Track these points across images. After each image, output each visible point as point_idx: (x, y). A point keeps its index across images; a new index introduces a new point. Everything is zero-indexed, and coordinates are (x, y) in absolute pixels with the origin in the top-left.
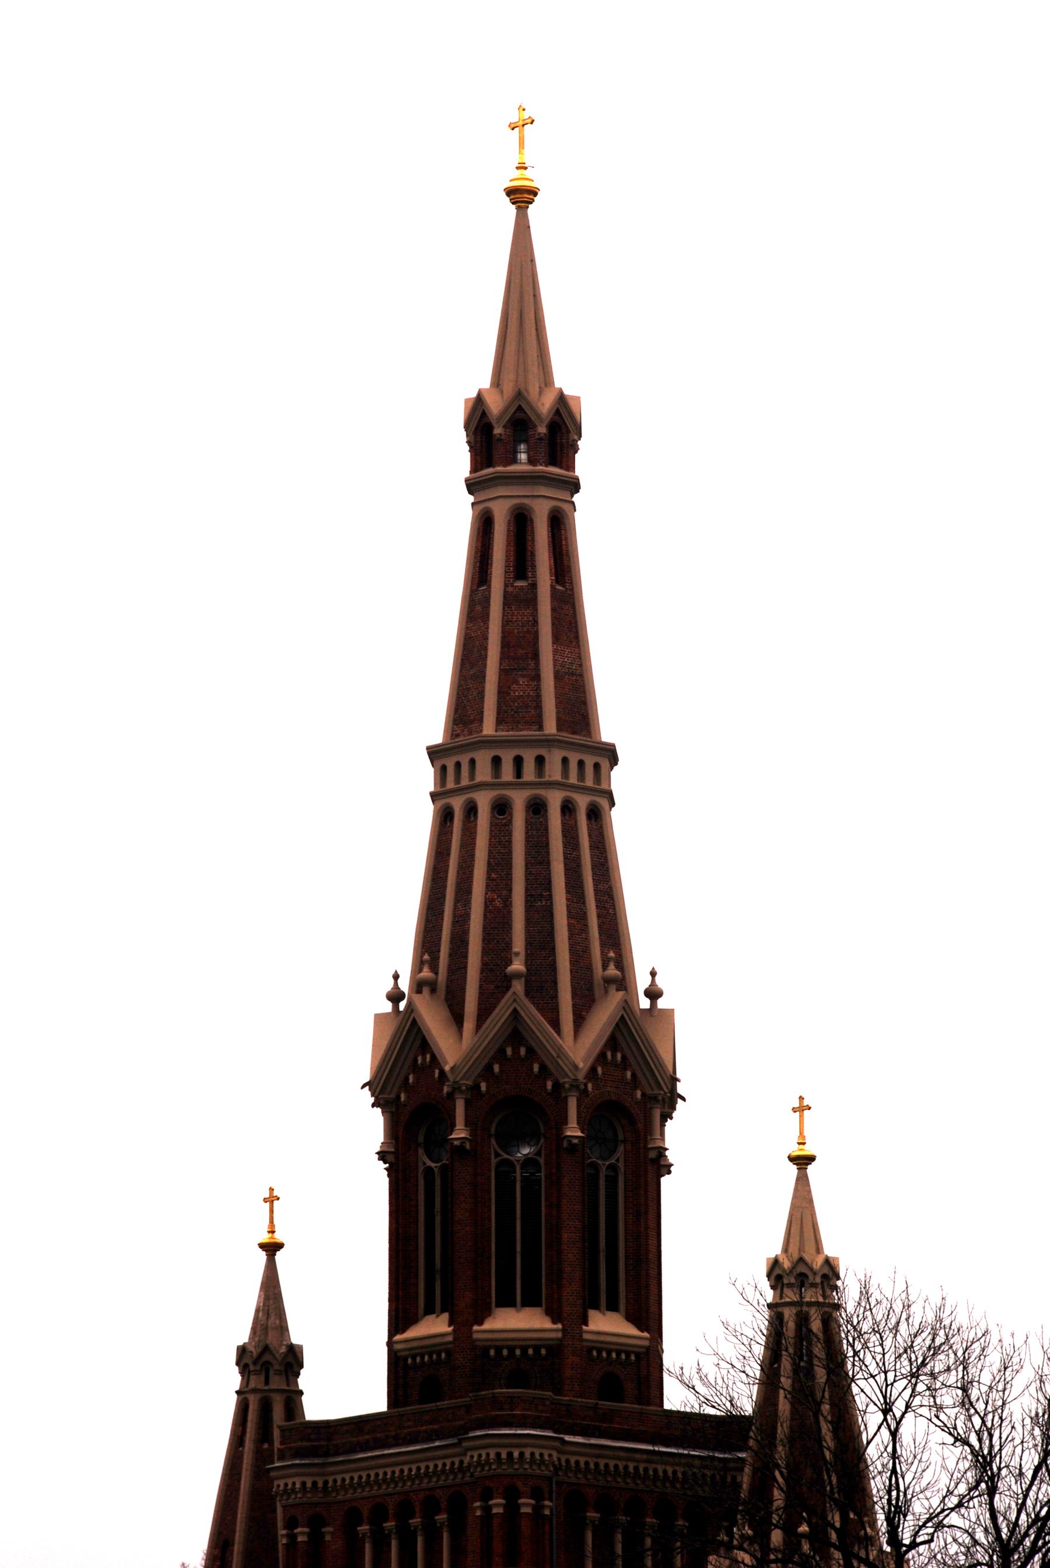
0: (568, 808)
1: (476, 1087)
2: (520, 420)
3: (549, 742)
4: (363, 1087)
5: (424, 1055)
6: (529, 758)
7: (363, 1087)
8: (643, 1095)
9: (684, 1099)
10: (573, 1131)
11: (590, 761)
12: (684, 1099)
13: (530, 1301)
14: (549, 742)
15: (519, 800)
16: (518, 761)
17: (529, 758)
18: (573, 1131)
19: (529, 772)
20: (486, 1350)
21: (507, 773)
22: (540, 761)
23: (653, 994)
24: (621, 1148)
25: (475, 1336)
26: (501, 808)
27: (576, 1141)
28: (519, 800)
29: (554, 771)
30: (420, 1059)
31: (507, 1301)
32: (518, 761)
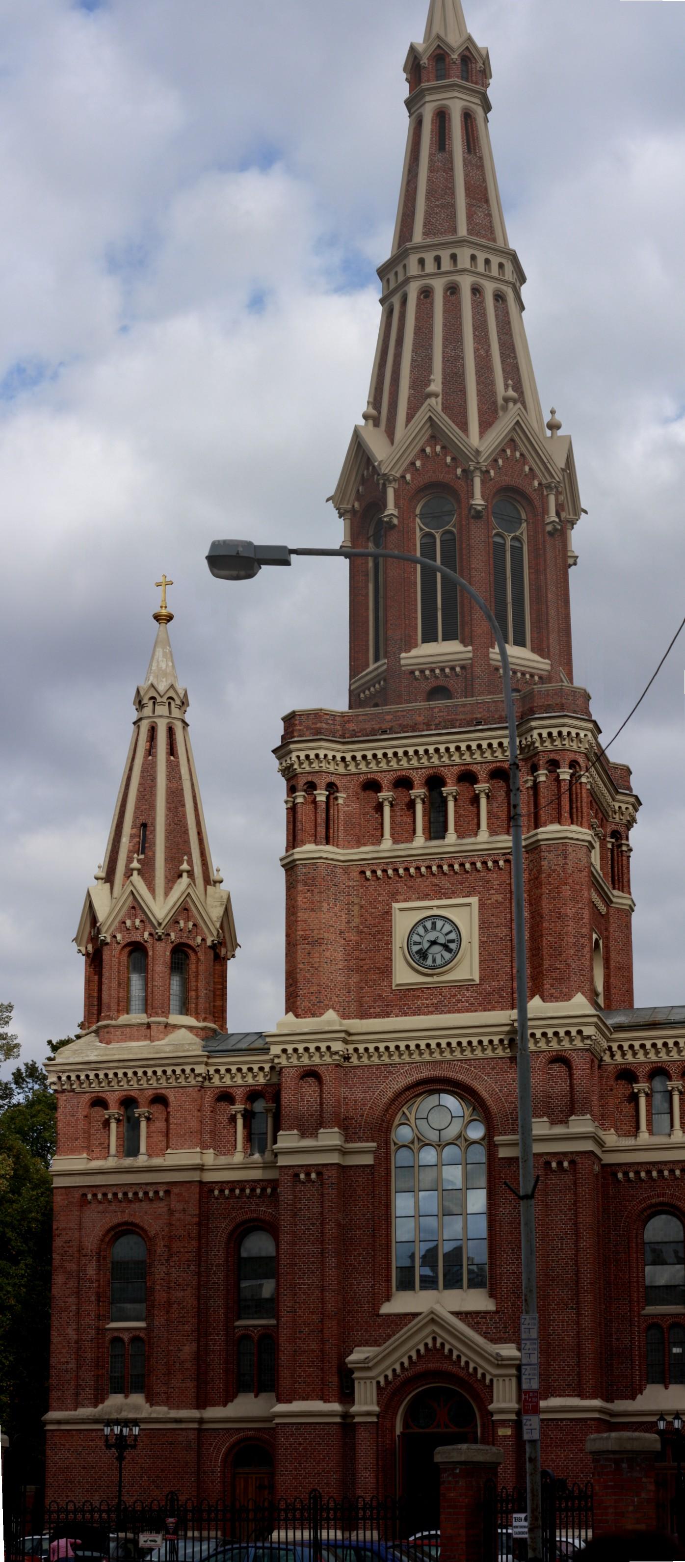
0: (476, 290)
1: (403, 477)
2: (440, 55)
3: (461, 243)
4: (328, 500)
5: (368, 469)
6: (445, 255)
7: (328, 500)
8: (540, 484)
9: (586, 512)
10: (478, 500)
11: (495, 261)
12: (586, 512)
13: (448, 636)
14: (461, 243)
15: (439, 286)
16: (438, 259)
17: (445, 255)
18: (478, 500)
19: (446, 265)
20: (412, 672)
21: (430, 267)
22: (454, 257)
23: (554, 426)
24: (524, 525)
25: (403, 662)
26: (426, 293)
27: (479, 508)
28: (439, 286)
29: (464, 261)
30: (365, 473)
31: (430, 637)
32: (438, 259)
